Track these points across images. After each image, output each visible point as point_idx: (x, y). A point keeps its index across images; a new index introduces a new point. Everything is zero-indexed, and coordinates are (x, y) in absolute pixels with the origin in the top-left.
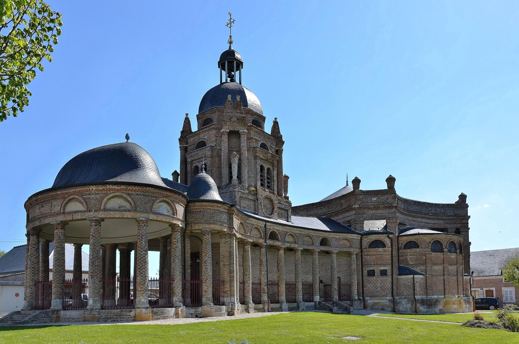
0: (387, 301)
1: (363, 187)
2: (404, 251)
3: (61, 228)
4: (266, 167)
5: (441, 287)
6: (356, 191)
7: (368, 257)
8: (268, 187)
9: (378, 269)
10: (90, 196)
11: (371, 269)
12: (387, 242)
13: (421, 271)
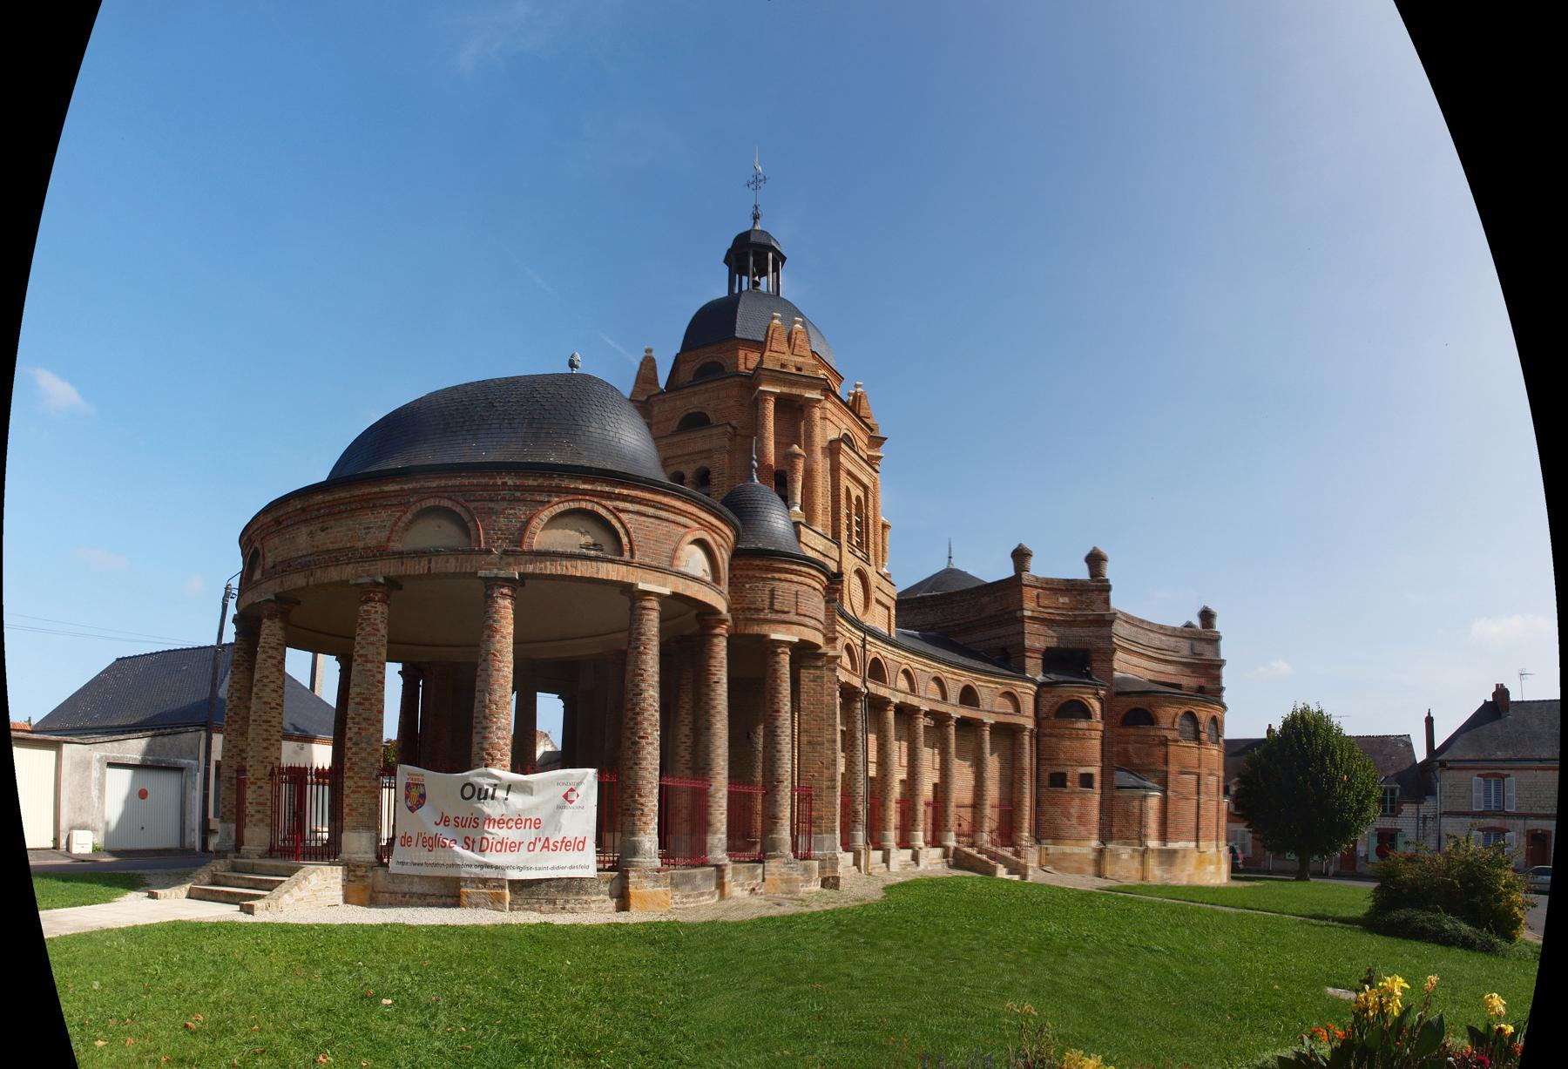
1: (1039, 568)
2: (1122, 731)
3: (382, 601)
5: (1193, 824)
6: (1024, 575)
7: (1054, 740)
8: (860, 545)
9: (1074, 772)
10: (492, 505)
11: (1060, 770)
12: (1096, 706)
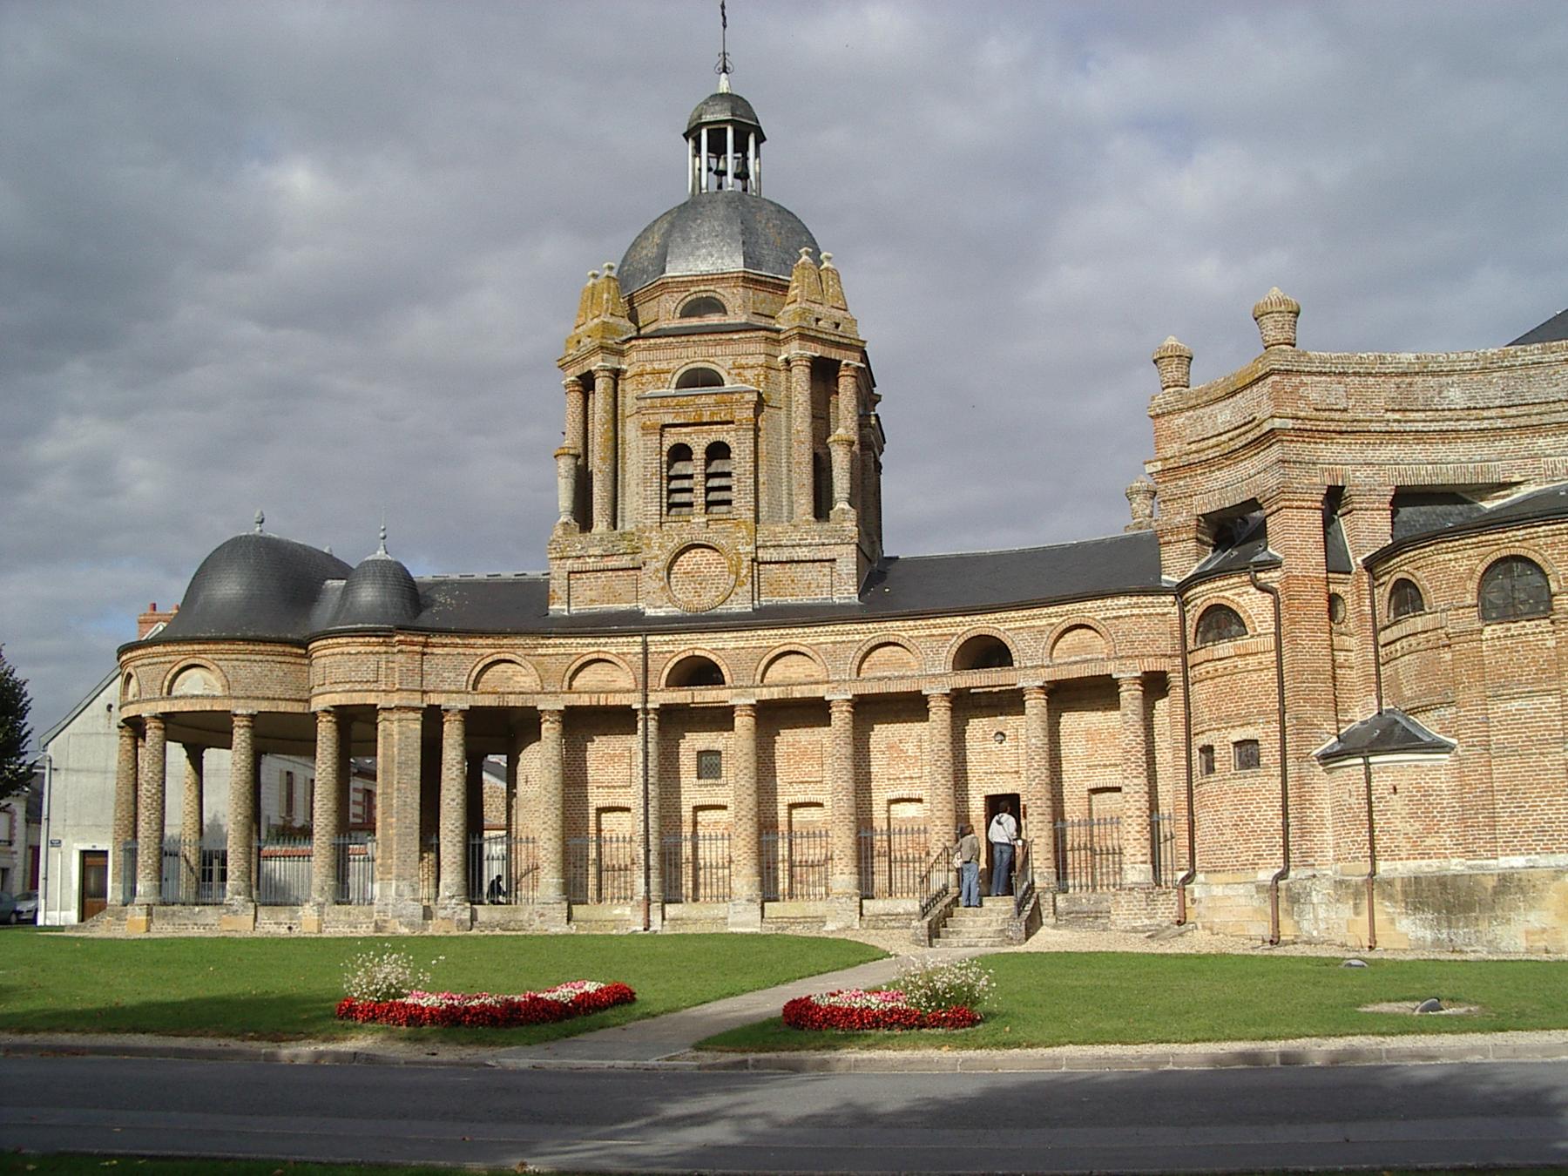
0: (1252, 888)
4: (699, 443)
9: (1224, 740)
13: (1444, 730)
